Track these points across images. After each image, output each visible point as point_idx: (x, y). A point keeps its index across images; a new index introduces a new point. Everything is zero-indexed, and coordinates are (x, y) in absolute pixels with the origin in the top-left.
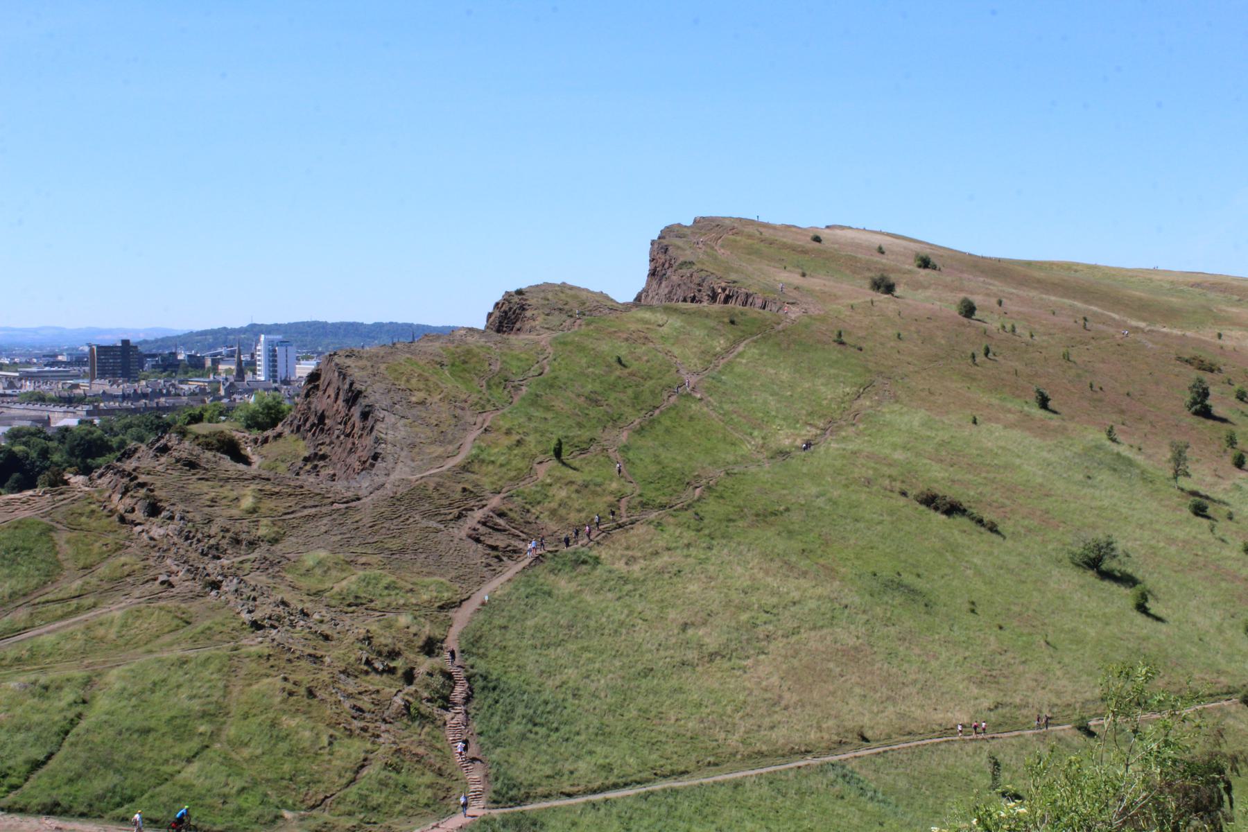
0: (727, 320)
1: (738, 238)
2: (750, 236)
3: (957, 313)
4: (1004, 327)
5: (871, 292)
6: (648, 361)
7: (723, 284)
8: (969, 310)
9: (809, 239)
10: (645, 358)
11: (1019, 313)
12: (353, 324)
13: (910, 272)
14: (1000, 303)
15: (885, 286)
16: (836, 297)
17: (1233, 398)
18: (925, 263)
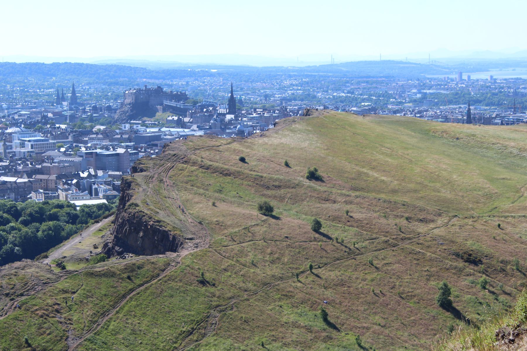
0: (125, 275)
1: (185, 166)
2: (194, 163)
3: (310, 227)
4: (337, 239)
5: (256, 212)
6: (49, 334)
7: (151, 223)
8: (317, 227)
9: (238, 158)
10: (48, 332)
11: (358, 221)
12: (36, 64)
13: (296, 186)
14: (347, 212)
15: (267, 210)
16: (226, 227)
17: (479, 286)
18: (313, 176)
